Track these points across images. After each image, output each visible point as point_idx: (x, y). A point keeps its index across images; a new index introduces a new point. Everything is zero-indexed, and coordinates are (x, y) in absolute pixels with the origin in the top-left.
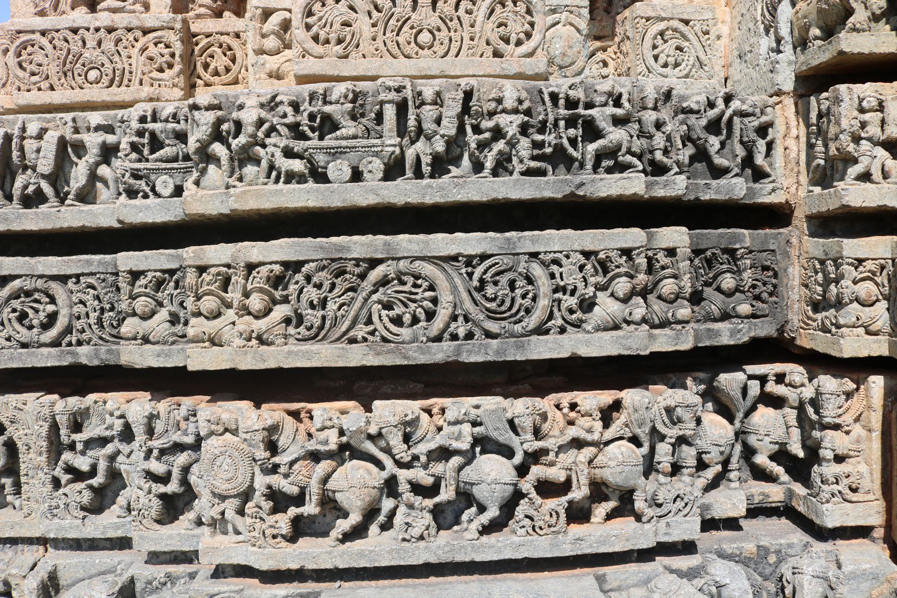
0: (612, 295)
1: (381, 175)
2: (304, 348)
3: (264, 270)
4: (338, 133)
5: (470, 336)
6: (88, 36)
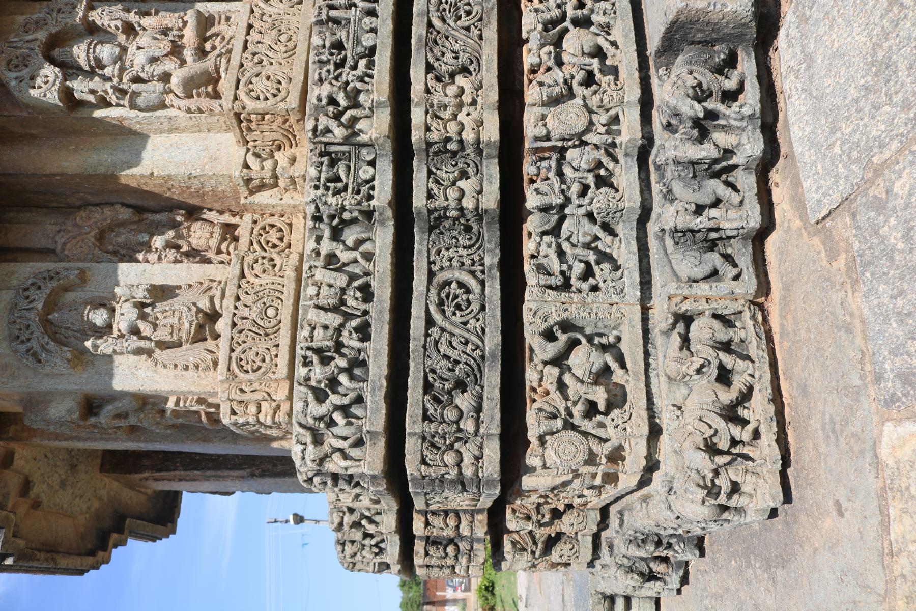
1: (374, 19)
2: (485, 67)
3: (430, 83)
4: (344, 40)
6: (240, 313)
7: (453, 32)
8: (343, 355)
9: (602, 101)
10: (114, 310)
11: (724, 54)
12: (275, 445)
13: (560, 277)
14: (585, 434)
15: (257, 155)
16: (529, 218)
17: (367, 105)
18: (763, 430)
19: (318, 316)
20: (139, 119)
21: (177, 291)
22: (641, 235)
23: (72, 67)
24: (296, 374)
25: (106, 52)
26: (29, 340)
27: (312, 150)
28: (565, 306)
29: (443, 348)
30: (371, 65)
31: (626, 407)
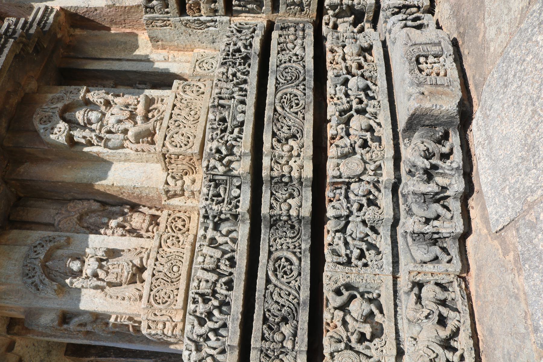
0: (293, 49)
3: (274, 143)
4: (227, 117)
5: (304, 85)
6: (157, 268)
7: (288, 115)
8: (216, 298)
9: (372, 157)
10: (84, 262)
11: (442, 132)
12: (172, 347)
13: (345, 258)
14: (358, 353)
15: (173, 177)
16: (328, 222)
17: (238, 154)
18: (466, 355)
19: (203, 274)
20: (108, 154)
21: (122, 253)
22: (393, 234)
23: (74, 123)
24: (188, 308)
25: (94, 116)
26: (33, 277)
27: (205, 178)
28: (348, 275)
29: (275, 297)
30: (241, 131)
31: (383, 337)
